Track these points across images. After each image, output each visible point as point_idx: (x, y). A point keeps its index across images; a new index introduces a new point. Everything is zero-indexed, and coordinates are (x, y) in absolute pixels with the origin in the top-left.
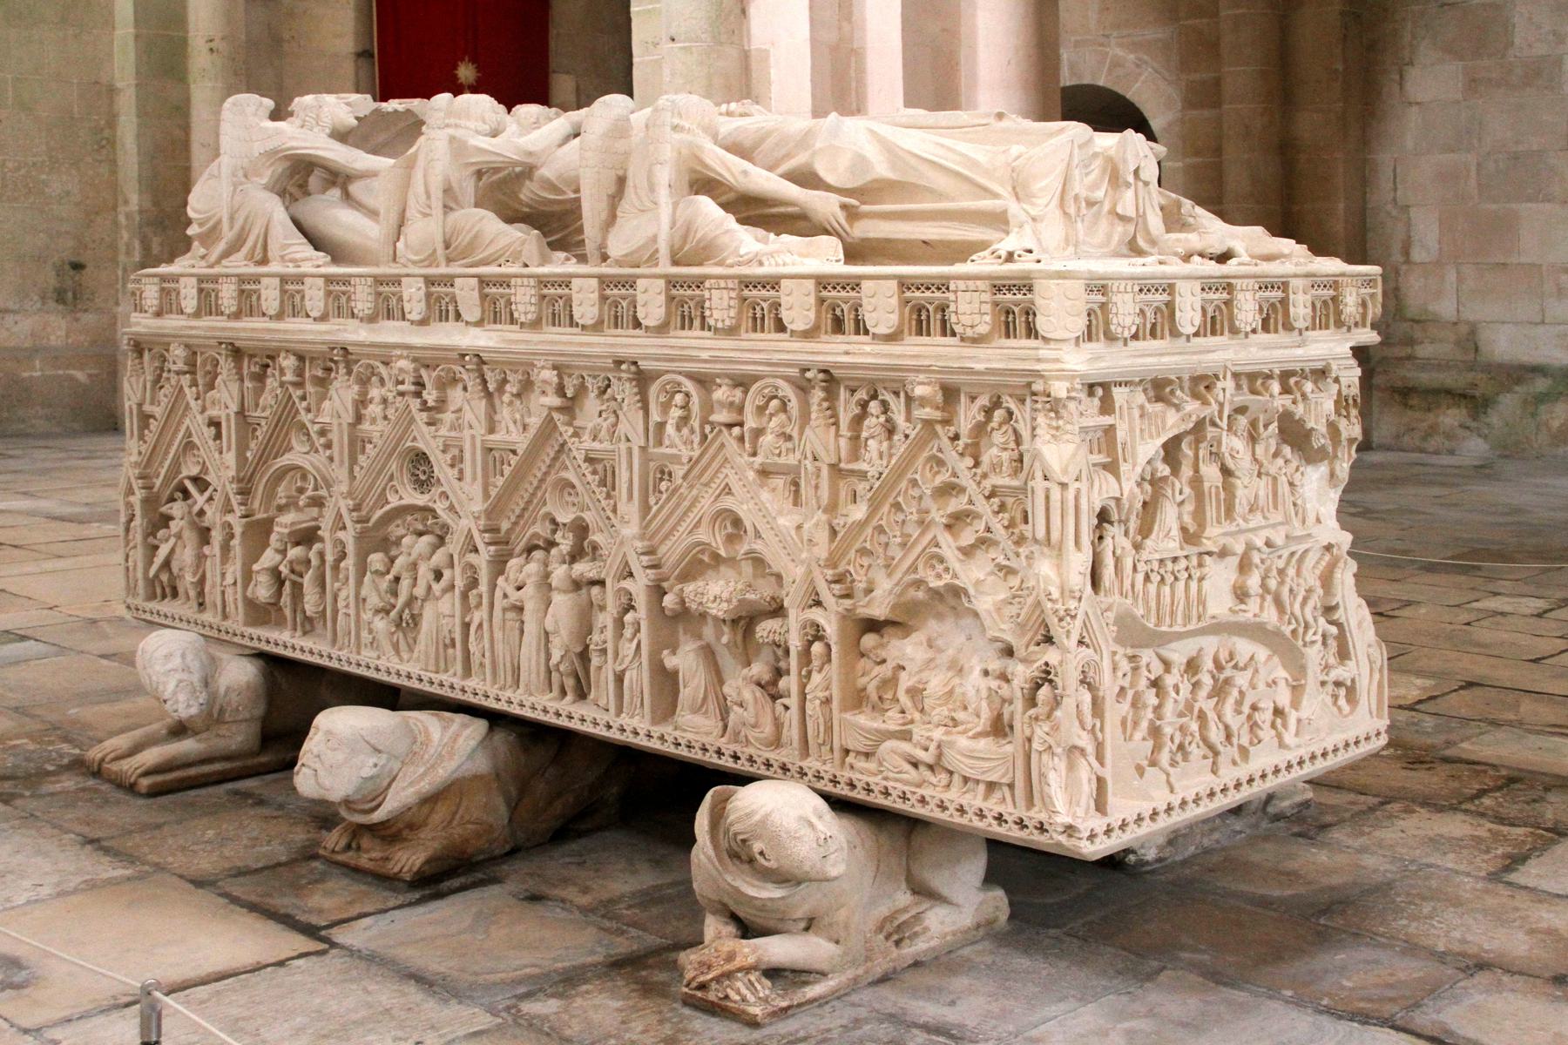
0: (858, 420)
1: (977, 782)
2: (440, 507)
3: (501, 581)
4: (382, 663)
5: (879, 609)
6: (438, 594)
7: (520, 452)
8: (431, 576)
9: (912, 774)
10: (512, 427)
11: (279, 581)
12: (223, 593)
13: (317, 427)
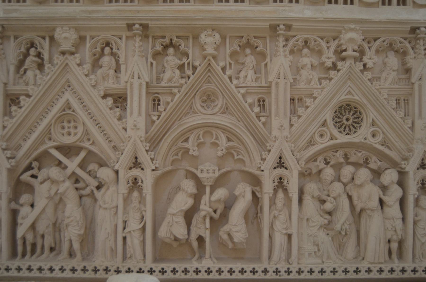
6: (391, 203)
8: (381, 193)
12: (125, 238)
13: (243, 91)
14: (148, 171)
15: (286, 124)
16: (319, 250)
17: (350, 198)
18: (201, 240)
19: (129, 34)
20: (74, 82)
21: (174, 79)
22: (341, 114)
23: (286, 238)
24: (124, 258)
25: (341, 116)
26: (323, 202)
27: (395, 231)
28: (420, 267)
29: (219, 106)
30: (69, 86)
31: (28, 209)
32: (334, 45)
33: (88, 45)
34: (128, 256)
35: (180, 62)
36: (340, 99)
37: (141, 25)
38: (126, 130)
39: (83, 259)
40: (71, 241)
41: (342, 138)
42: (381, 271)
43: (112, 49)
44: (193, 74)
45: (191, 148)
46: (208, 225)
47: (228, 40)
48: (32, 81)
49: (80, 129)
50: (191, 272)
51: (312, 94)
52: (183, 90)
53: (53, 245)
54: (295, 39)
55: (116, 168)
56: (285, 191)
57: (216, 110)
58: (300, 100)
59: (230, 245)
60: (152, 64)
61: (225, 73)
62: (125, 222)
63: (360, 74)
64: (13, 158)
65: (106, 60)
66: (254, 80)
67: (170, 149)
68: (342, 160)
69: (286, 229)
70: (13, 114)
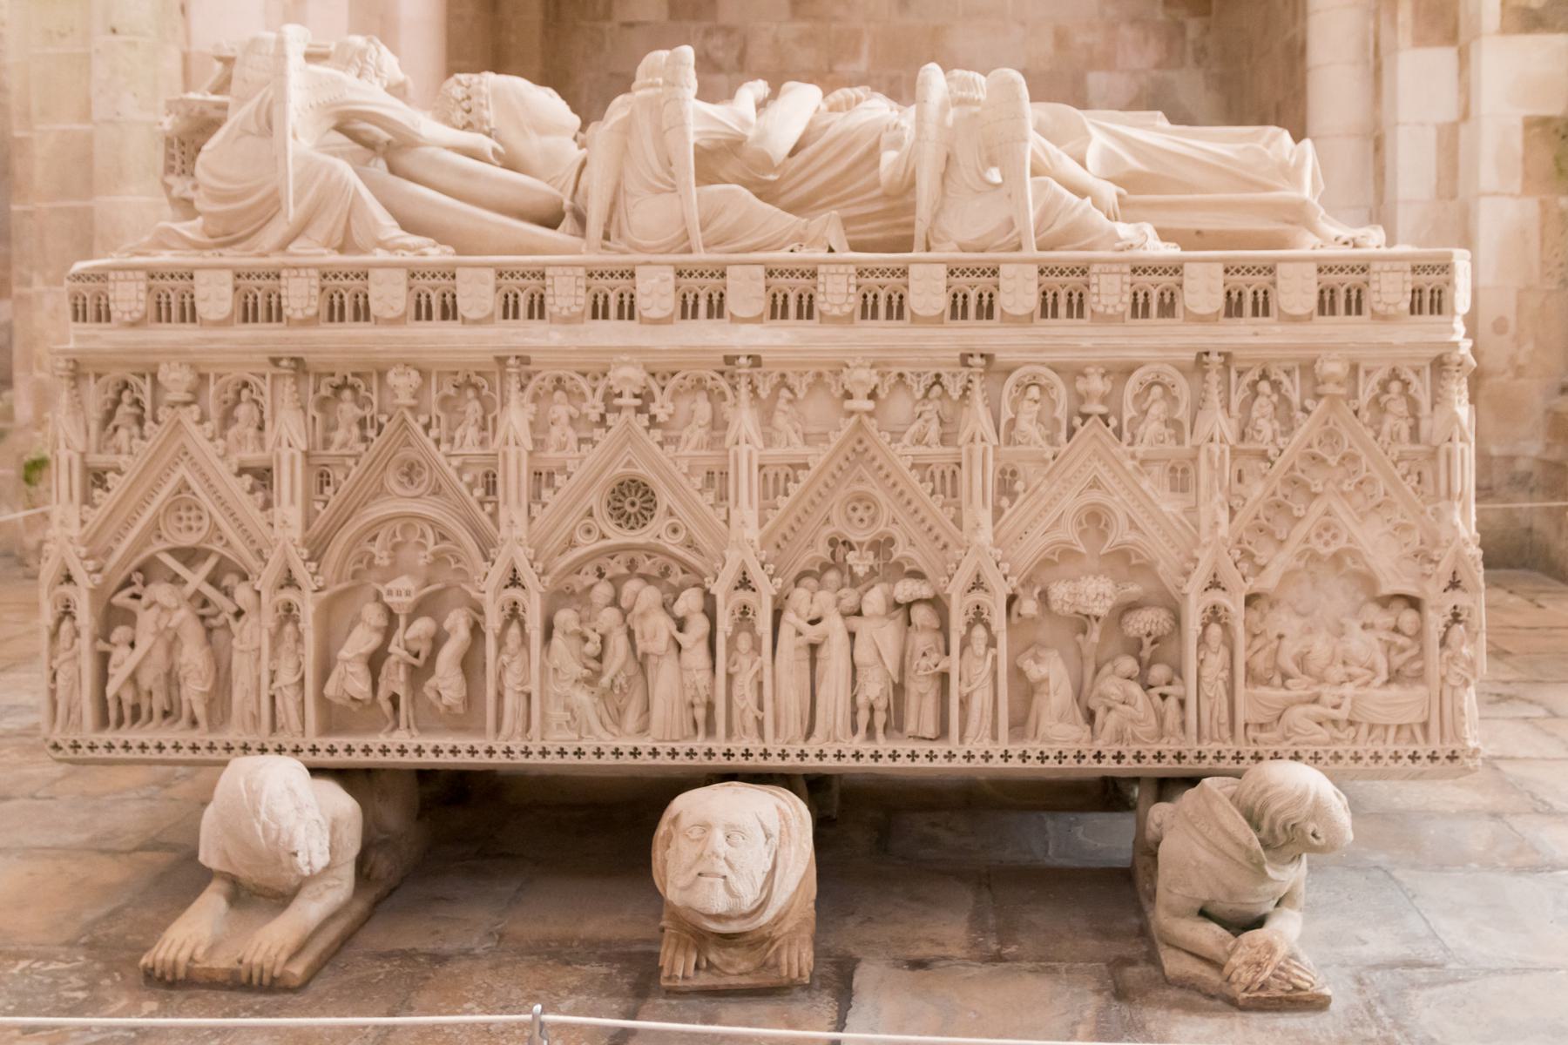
0: (1247, 406)
1: (1386, 727)
2: (672, 544)
3: (789, 617)
4: (588, 745)
5: (1268, 582)
7: (815, 468)
8: (673, 627)
9: (1324, 734)
10: (794, 438)
11: (375, 662)
12: (273, 698)
13: (456, 462)
14: (308, 594)
15: (520, 517)
16: (575, 719)
17: (630, 634)
18: (394, 699)
19: (275, 370)
20: (191, 448)
21: (351, 443)
22: (624, 494)
23: (524, 698)
24: (274, 728)
25: (622, 498)
26: (586, 640)
27: (696, 689)
28: (737, 748)
29: (425, 484)
30: (186, 453)
31: (126, 650)
32: (601, 386)
33: (212, 389)
34: (279, 725)
35: (360, 413)
36: (616, 472)
37: (292, 359)
38: (272, 525)
39: (212, 728)
40: (190, 701)
41: (619, 536)
42: (673, 753)
43: (252, 391)
44: (379, 434)
45: (377, 554)
46: (402, 676)
47: (434, 380)
48: (125, 448)
49: (206, 522)
50: (375, 751)
51: (565, 467)
52: (361, 461)
53: (167, 708)
54: (540, 376)
55: (257, 588)
56: (522, 624)
57: (421, 490)
58: (551, 475)
59: (442, 709)
60: (314, 419)
61: (427, 434)
62: (273, 673)
63: (643, 433)
64: (99, 571)
65: (243, 411)
66: (476, 443)
67: (349, 553)
68: (624, 571)
69: (522, 684)
70: (97, 501)
